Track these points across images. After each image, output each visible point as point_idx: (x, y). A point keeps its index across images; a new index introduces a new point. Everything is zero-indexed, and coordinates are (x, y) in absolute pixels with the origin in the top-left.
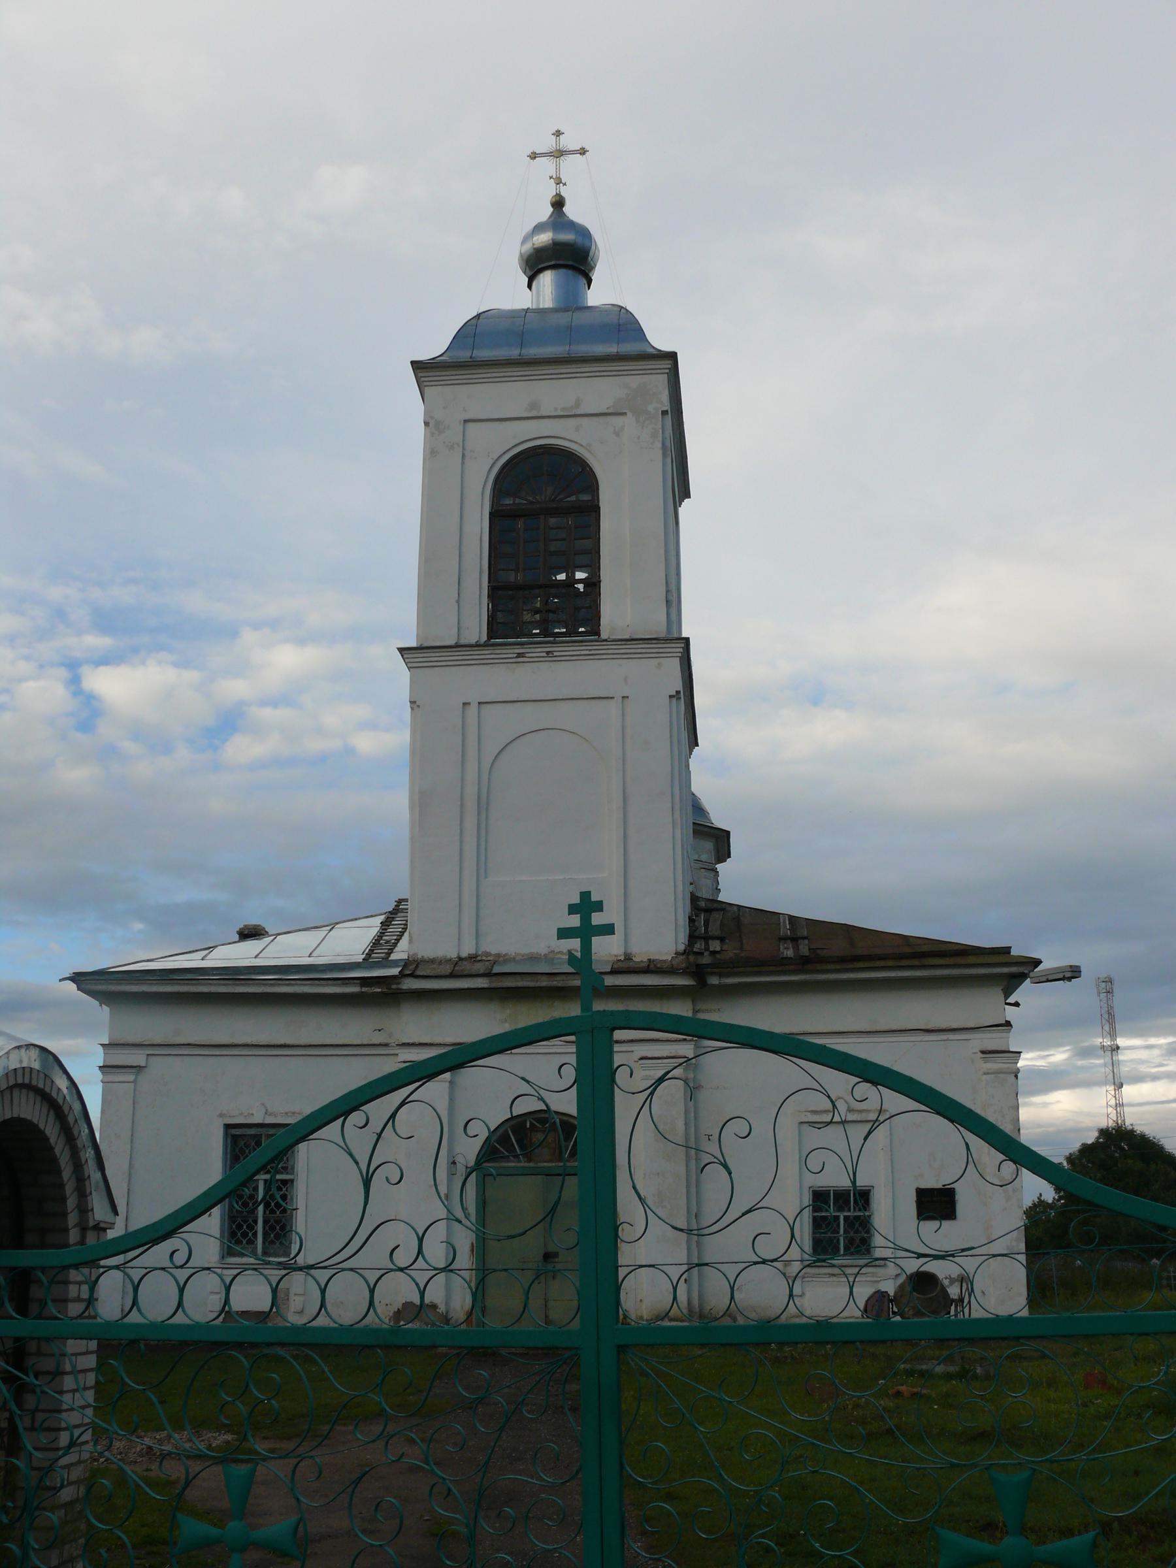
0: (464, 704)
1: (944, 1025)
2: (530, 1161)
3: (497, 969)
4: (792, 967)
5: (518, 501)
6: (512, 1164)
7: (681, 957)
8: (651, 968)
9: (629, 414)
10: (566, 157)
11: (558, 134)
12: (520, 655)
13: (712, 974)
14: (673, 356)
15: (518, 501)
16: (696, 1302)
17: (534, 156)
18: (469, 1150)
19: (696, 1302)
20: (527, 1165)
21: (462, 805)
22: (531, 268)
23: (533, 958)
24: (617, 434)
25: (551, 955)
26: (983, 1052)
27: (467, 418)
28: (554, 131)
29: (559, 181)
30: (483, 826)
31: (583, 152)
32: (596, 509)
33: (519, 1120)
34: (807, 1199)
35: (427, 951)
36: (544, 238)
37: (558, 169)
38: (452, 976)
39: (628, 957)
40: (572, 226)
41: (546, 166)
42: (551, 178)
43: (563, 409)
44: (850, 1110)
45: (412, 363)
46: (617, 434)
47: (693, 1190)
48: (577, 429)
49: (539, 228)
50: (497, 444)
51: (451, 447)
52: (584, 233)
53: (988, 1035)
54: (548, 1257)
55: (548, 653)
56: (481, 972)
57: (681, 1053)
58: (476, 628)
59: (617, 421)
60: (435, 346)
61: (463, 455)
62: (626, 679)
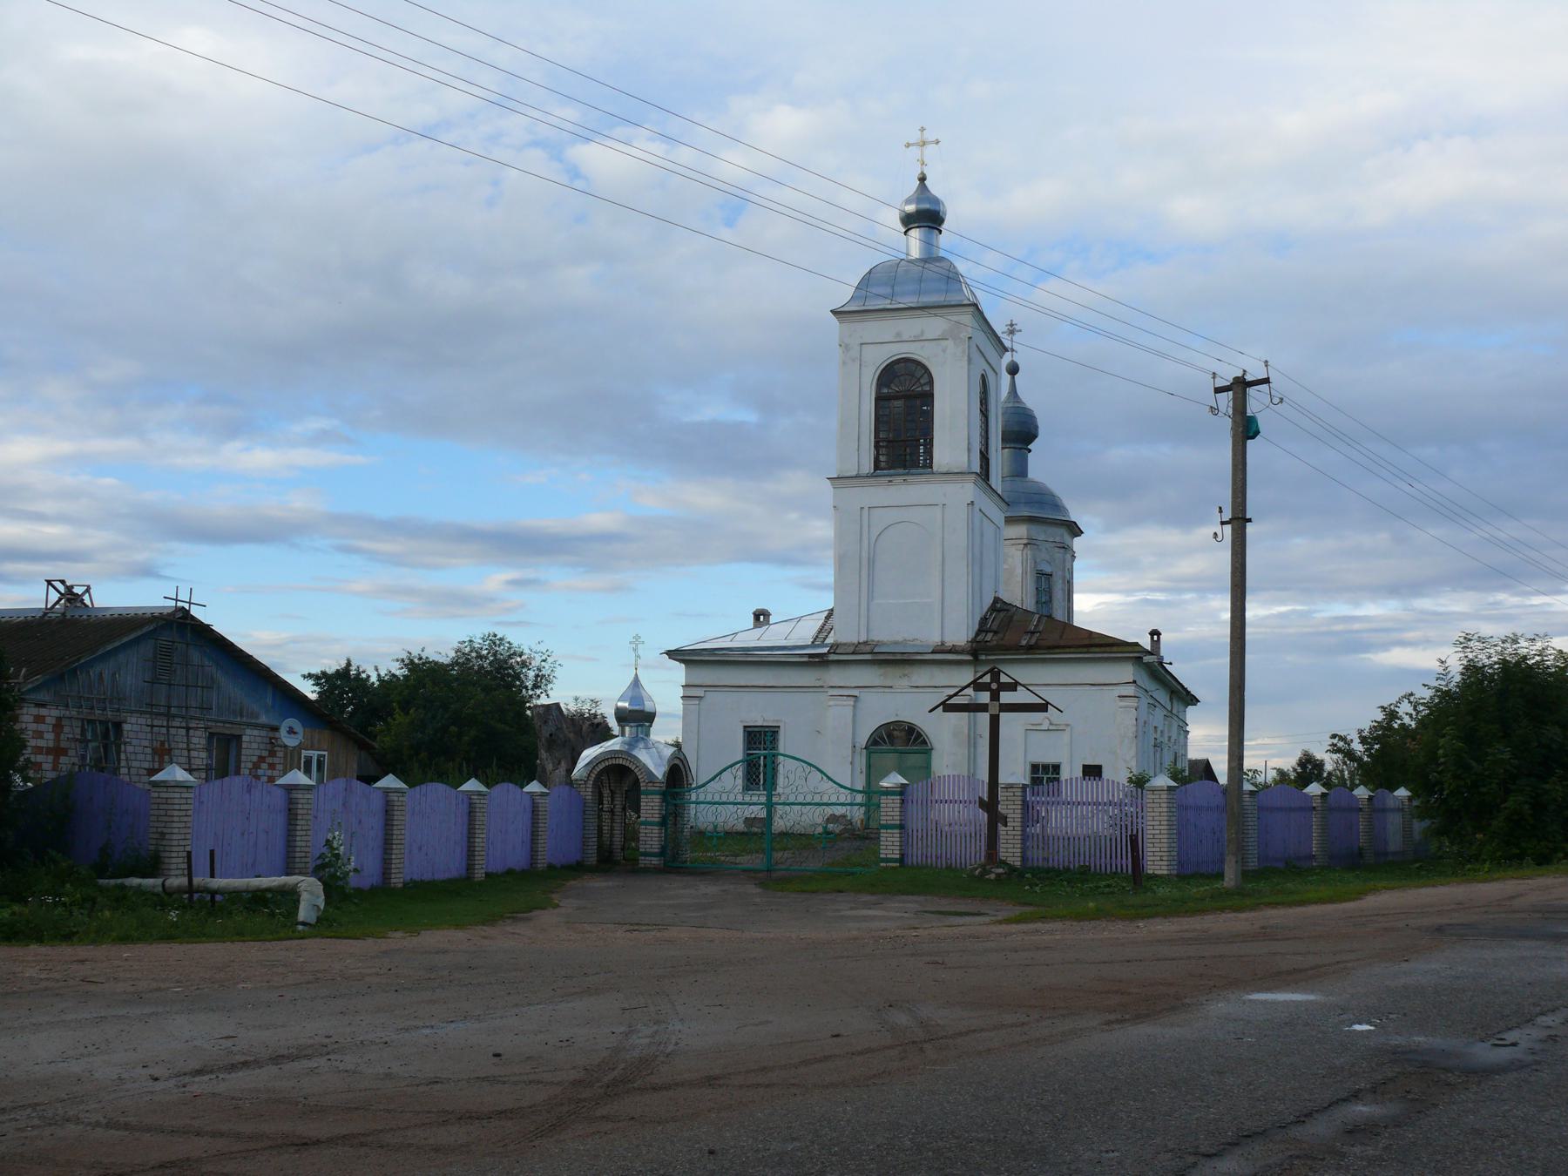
8: (953, 650)
18: (863, 738)
24: (944, 351)
34: (1028, 768)
35: (842, 640)
36: (911, 208)
39: (943, 644)
41: (915, 150)
49: (908, 202)
52: (937, 201)
58: (868, 466)
59: (944, 343)
60: (843, 295)
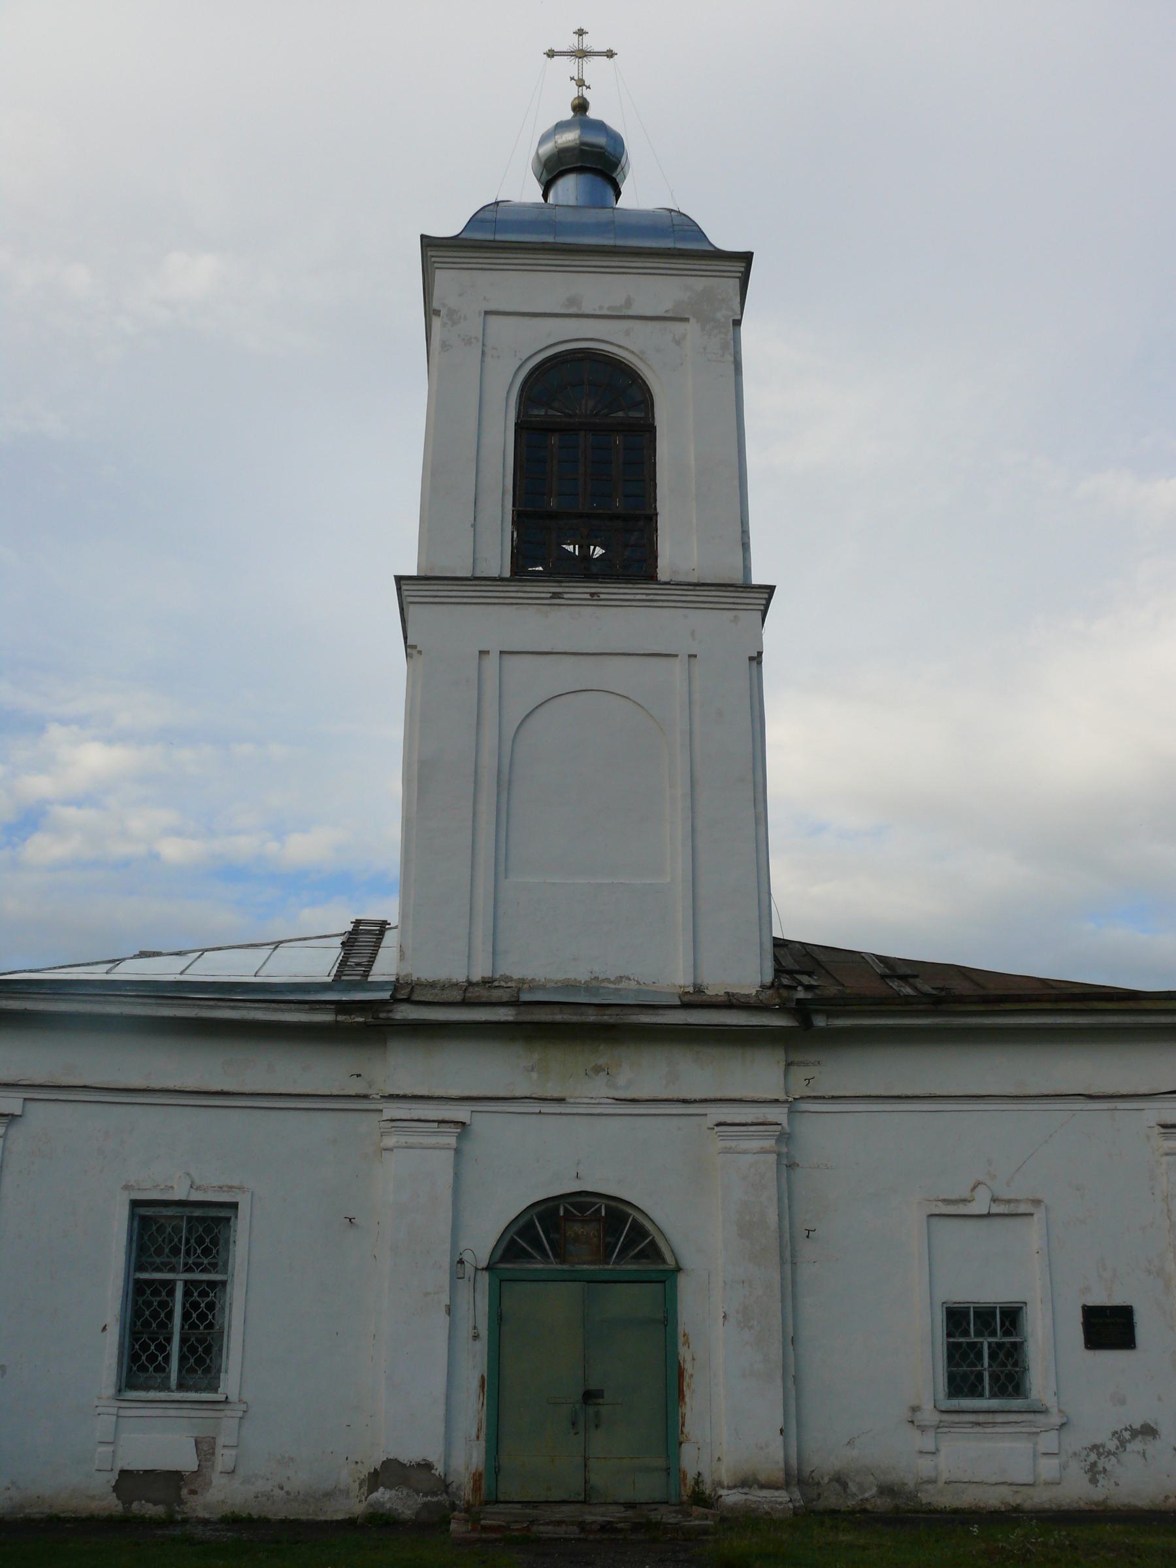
0: (481, 652)
1: (1110, 1090)
2: (563, 1262)
3: (525, 997)
4: (921, 1007)
5: (551, 412)
6: (540, 1266)
7: (770, 992)
8: (731, 1003)
9: (692, 320)
10: (590, 58)
11: (581, 33)
12: (556, 595)
13: (818, 1012)
14: (746, 258)
15: (551, 412)
16: (794, 1462)
17: (551, 54)
18: (482, 1241)
19: (794, 1462)
20: (559, 1267)
21: (476, 782)
22: (549, 172)
23: (569, 986)
24: (678, 343)
25: (594, 983)
26: (1164, 1126)
27: (492, 307)
28: (576, 29)
29: (581, 83)
30: (504, 806)
31: (610, 54)
32: (651, 430)
33: (551, 1204)
34: (940, 1317)
35: (425, 970)
36: (570, 137)
37: (580, 69)
38: (465, 1003)
39: (699, 989)
40: (600, 126)
41: (569, 66)
42: (572, 79)
43: (609, 308)
44: (994, 1200)
45: (423, 237)
46: (678, 343)
47: (789, 1303)
48: (627, 333)
49: (561, 127)
50: (525, 344)
51: (468, 342)
52: (617, 140)
53: (1167, 1105)
54: (589, 1396)
55: (592, 594)
56: (505, 999)
57: (771, 1119)
58: (496, 558)
59: (678, 327)
60: (450, 226)
61: (483, 353)
62: (693, 634)
